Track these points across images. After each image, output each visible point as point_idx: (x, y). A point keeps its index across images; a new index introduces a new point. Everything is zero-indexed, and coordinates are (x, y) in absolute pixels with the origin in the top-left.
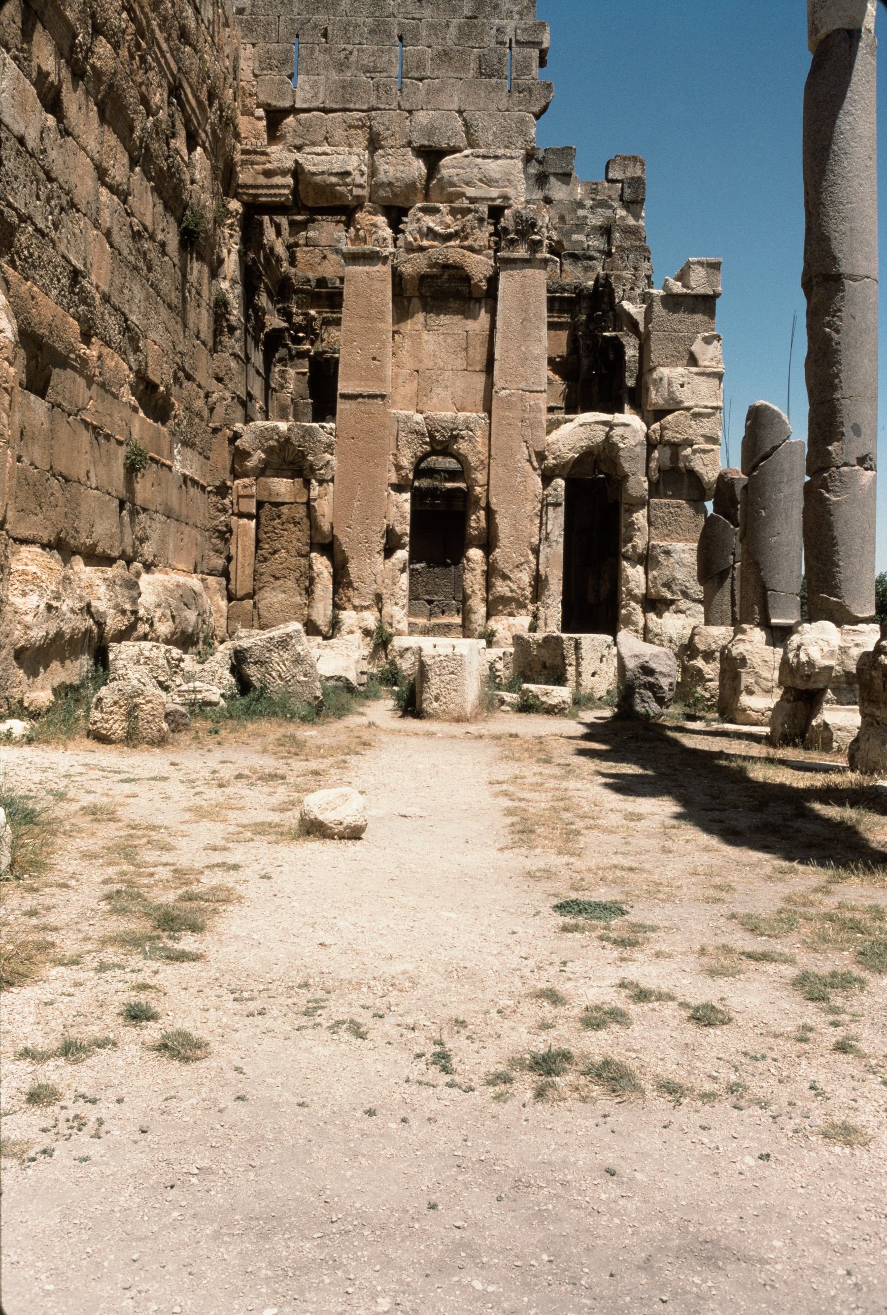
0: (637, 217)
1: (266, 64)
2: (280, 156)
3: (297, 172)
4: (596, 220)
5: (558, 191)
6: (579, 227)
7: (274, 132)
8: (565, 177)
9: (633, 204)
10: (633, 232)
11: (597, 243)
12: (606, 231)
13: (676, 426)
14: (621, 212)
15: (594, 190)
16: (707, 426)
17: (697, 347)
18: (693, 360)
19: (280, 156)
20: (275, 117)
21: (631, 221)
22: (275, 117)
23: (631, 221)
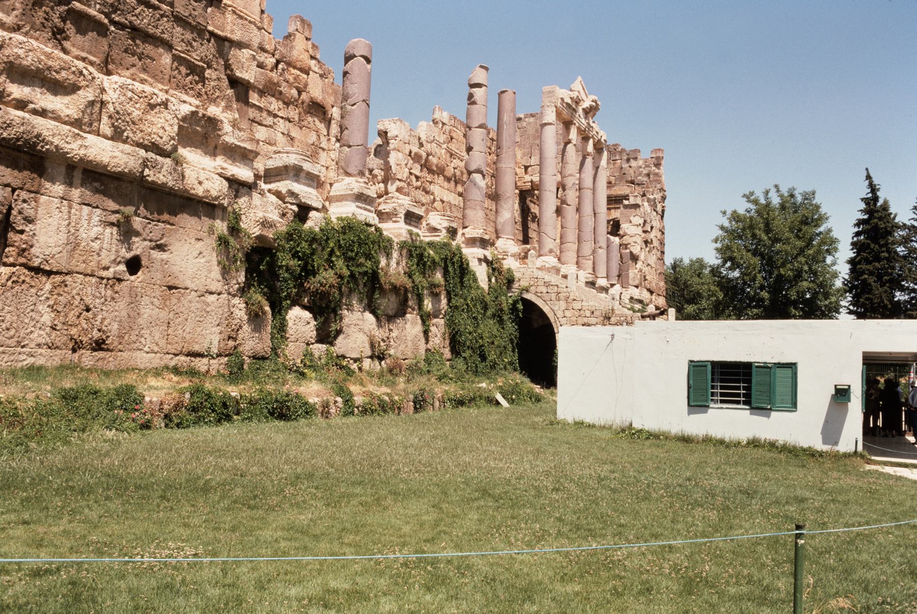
0: (659, 169)
1: (524, 155)
2: (528, 178)
3: (532, 182)
4: (645, 172)
5: (633, 163)
6: (640, 175)
7: (526, 172)
8: (636, 159)
9: (658, 165)
10: (657, 174)
11: (645, 179)
12: (648, 175)
13: (626, 240)
14: (654, 168)
15: (646, 161)
16: (634, 239)
17: (632, 218)
18: (631, 222)
19: (528, 178)
20: (526, 168)
21: (657, 171)
22: (526, 168)
23: (657, 171)
